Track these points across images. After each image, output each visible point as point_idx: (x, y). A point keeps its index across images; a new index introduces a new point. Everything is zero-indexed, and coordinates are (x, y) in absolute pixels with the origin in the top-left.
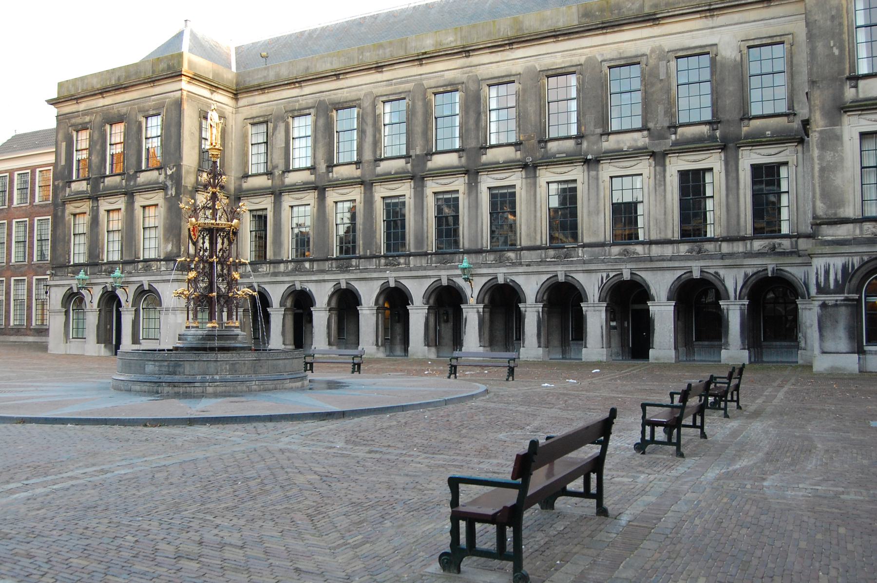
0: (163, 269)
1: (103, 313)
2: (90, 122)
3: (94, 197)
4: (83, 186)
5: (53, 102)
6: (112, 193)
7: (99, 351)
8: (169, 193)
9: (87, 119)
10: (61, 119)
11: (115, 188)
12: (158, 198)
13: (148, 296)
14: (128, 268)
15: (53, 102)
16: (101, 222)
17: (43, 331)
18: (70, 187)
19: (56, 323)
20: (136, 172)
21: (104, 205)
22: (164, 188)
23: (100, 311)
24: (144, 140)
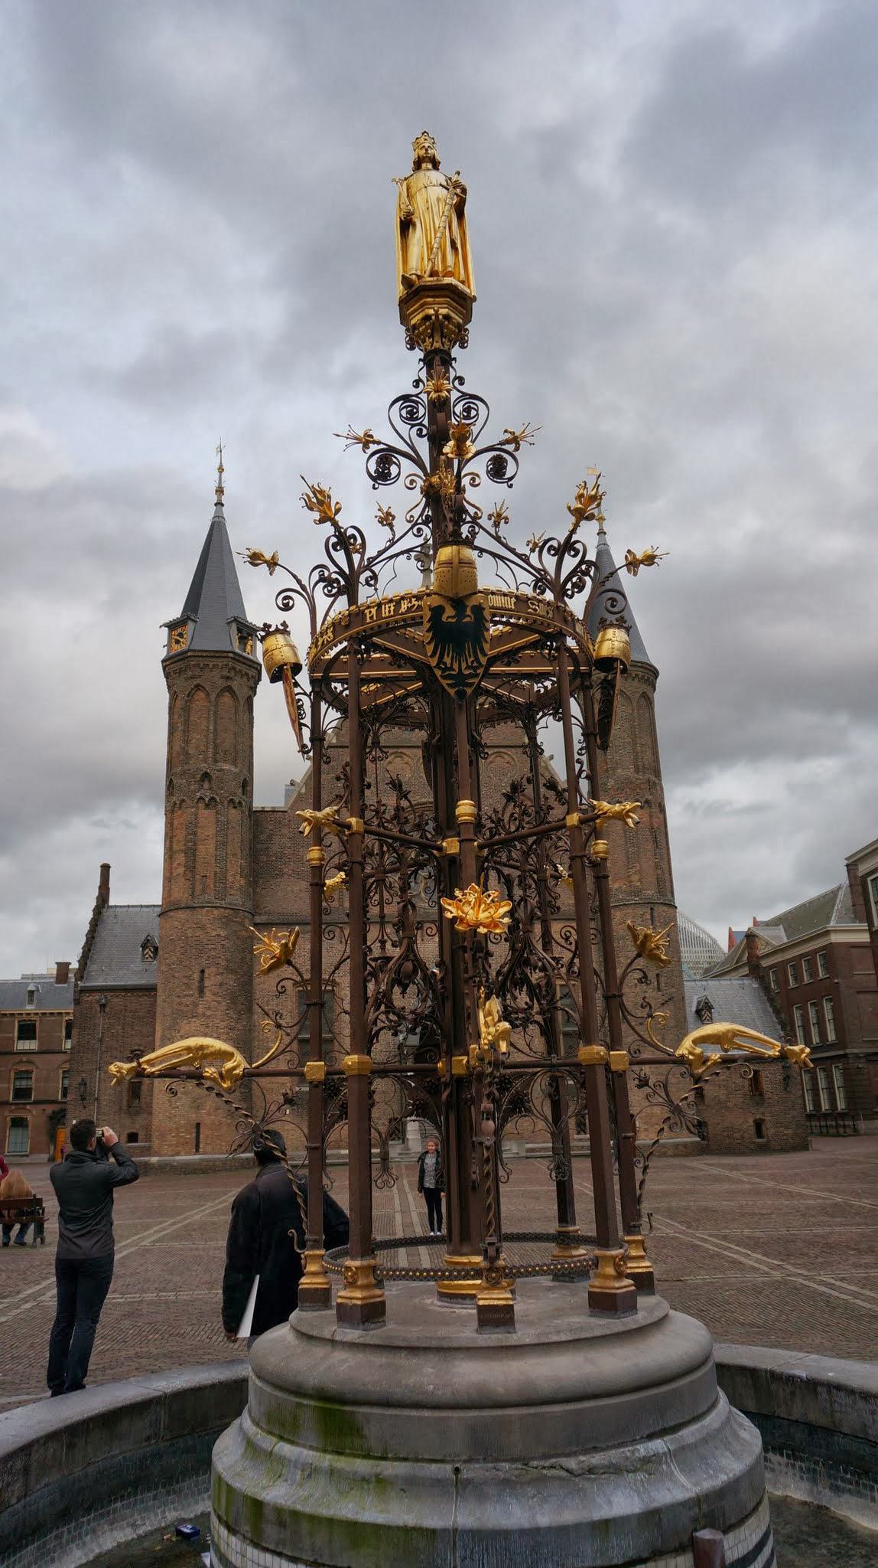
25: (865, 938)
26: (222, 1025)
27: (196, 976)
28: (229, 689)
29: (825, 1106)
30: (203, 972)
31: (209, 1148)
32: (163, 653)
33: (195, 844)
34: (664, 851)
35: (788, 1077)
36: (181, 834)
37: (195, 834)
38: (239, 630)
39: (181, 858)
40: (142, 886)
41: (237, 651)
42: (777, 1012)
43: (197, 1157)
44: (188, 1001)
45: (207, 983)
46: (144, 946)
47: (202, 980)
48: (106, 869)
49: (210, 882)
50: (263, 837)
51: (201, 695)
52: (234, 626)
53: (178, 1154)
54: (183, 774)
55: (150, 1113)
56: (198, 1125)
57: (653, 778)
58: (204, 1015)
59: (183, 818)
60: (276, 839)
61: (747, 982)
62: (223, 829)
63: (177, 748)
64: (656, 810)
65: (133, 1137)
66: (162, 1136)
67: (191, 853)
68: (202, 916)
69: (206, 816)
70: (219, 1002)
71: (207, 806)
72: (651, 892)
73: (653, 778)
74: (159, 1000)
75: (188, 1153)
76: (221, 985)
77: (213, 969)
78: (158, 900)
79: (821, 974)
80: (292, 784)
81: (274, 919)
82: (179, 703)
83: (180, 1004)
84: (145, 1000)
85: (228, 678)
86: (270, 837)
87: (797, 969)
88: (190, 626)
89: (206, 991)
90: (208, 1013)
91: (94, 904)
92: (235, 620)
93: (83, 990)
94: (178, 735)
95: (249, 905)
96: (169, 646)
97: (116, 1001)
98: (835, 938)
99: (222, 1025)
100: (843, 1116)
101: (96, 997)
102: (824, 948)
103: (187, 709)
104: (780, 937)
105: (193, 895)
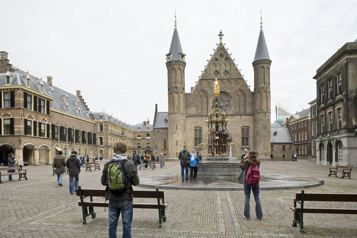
0: (343, 132)
1: (329, 150)
3: (325, 109)
4: (322, 105)
5: (314, 78)
6: (329, 106)
7: (327, 164)
8: (344, 102)
11: (330, 103)
12: (340, 105)
13: (339, 143)
14: (334, 133)
15: (314, 78)
16: (327, 117)
17: (315, 157)
18: (320, 106)
20: (335, 96)
21: (328, 111)
22: (342, 100)
23: (328, 149)
24: (338, 83)
27: (176, 126)
28: (180, 69)
29: (303, 153)
30: (177, 125)
32: (166, 61)
36: (171, 99)
38: (181, 55)
40: (164, 108)
41: (181, 60)
42: (291, 134)
45: (178, 127)
46: (165, 120)
47: (177, 127)
48: (156, 105)
49: (178, 108)
50: (187, 99)
55: (168, 151)
57: (268, 86)
58: (177, 133)
60: (189, 99)
61: (285, 128)
65: (165, 155)
66: (171, 154)
67: (173, 103)
68: (176, 115)
69: (176, 95)
71: (176, 93)
72: (265, 110)
78: (167, 110)
81: (190, 115)
82: (170, 72)
85: (179, 66)
87: (301, 124)
88: (171, 55)
91: (155, 112)
93: (154, 129)
95: (185, 113)
97: (161, 131)
100: (306, 155)
101: (157, 130)
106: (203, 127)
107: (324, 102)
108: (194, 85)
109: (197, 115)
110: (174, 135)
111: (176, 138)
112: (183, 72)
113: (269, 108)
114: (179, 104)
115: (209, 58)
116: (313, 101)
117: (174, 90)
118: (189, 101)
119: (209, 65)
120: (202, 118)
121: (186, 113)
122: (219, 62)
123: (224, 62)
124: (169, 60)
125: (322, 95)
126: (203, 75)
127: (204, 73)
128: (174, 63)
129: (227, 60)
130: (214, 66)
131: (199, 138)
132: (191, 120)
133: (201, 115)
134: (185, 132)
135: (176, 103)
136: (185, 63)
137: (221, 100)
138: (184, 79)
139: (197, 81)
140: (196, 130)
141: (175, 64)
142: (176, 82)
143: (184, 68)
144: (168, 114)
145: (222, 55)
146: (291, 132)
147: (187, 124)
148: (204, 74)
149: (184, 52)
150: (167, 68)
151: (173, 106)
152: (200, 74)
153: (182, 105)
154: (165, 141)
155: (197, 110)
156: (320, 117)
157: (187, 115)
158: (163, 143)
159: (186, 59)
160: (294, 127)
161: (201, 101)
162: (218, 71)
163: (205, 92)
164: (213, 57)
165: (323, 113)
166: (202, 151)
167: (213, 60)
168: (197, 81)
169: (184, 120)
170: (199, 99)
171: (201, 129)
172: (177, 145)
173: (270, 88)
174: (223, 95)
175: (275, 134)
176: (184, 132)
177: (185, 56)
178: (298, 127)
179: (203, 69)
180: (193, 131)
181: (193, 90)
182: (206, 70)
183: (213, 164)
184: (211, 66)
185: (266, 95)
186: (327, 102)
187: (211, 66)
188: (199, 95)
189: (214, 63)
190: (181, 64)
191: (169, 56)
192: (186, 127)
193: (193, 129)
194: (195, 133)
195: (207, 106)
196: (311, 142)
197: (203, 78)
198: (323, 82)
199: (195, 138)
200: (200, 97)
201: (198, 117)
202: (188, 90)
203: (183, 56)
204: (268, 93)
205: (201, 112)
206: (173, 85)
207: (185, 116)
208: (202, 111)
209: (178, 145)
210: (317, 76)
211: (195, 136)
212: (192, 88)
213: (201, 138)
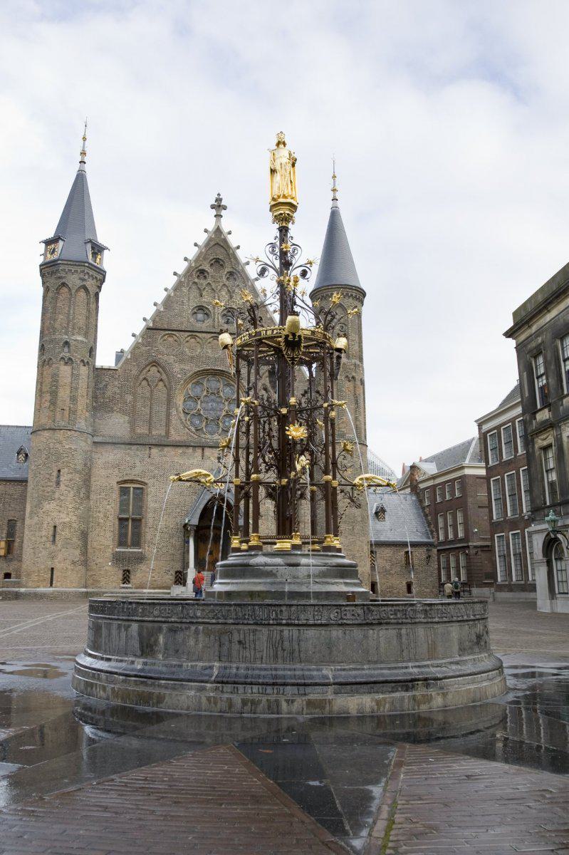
2: (543, 342)
4: (544, 415)
9: (540, 340)
10: (519, 348)
18: (535, 419)
19: (540, 576)
25: (483, 472)
26: (70, 506)
27: (55, 474)
30: (59, 471)
31: (58, 584)
32: (41, 260)
33: (57, 388)
34: (362, 410)
35: (430, 556)
36: (48, 380)
37: (57, 381)
38: (93, 248)
39: (48, 397)
41: (91, 261)
42: (426, 516)
43: (51, 589)
44: (49, 489)
46: (18, 453)
47: (58, 476)
49: (66, 413)
50: (101, 386)
51: (65, 290)
52: (89, 246)
53: (39, 587)
54: (51, 341)
55: (21, 561)
56: (52, 569)
57: (358, 362)
59: (48, 371)
60: (109, 387)
61: (409, 497)
62: (75, 376)
63: (47, 324)
64: (359, 383)
66: (28, 575)
67: (54, 394)
68: (59, 435)
69: (65, 371)
70: (69, 492)
71: (66, 363)
73: (358, 362)
74: (29, 489)
75: (44, 587)
76: (71, 480)
77: (66, 470)
78: (31, 424)
79: (457, 494)
80: (122, 351)
81: (108, 440)
82: (50, 294)
83: (44, 491)
84: (19, 488)
85: (83, 280)
86: (106, 386)
87: (443, 490)
88: (61, 243)
89: (61, 483)
90: (62, 498)
92: (90, 241)
94: (48, 315)
95: (90, 430)
96: (45, 255)
98: (467, 472)
99: (70, 506)
102: (460, 477)
103: (55, 299)
104: (431, 469)
105: (54, 421)
106: (150, 482)
107: (546, 405)
108: (127, 344)
109: (133, 441)
110: (48, 506)
111: (55, 514)
112: (92, 300)
113: (363, 431)
114: (73, 399)
115: (182, 267)
116: (492, 413)
117: (60, 353)
118: (109, 393)
119: (177, 287)
120: (147, 452)
121: (94, 431)
122: (209, 280)
123: (227, 283)
124: (50, 258)
125: (540, 383)
126: (158, 313)
127: (162, 309)
128: (67, 268)
129: (235, 279)
130: (195, 293)
131: (134, 520)
132: (109, 456)
133: (147, 441)
134: (88, 498)
135: (64, 394)
136: (103, 274)
137: (213, 397)
138: (97, 320)
139: (137, 333)
140: (124, 491)
141: (71, 273)
142: (67, 328)
143: (100, 288)
144: (31, 430)
145: (217, 262)
146: (427, 510)
147: (94, 470)
148: (160, 312)
149: (101, 240)
150: (44, 283)
151: (53, 403)
152: (150, 312)
153: (83, 402)
154: (12, 525)
155: (133, 424)
156: (537, 454)
157: (96, 439)
158: (5, 532)
159: (108, 262)
160: (435, 494)
161: (148, 394)
162: (207, 308)
163: (160, 369)
164: (193, 265)
165: (551, 440)
166: (143, 567)
167: (191, 275)
168: (137, 333)
169: (86, 452)
170: (143, 390)
171: (142, 488)
172: (54, 540)
173: (363, 369)
174: (219, 381)
175: (380, 513)
176: (82, 495)
177: (106, 252)
178: (436, 500)
179: (161, 297)
180: (115, 495)
181: (124, 359)
182: (168, 302)
183: (247, 601)
184: (185, 290)
185: (352, 388)
186: (562, 405)
187: (185, 290)
188: (141, 377)
189: (195, 283)
190: (91, 273)
191: (53, 246)
192: (93, 479)
193: (116, 487)
194: (121, 502)
195: (168, 415)
196: (492, 539)
197: (159, 326)
198: (540, 344)
199: (121, 520)
200: (144, 383)
201: (135, 447)
202: (105, 358)
203: (98, 249)
204: (358, 383)
205: (147, 432)
206: (58, 336)
207: (89, 441)
208: (150, 432)
209: (59, 543)
210: (517, 330)
211: (122, 511)
212: (119, 355)
213: (140, 520)
